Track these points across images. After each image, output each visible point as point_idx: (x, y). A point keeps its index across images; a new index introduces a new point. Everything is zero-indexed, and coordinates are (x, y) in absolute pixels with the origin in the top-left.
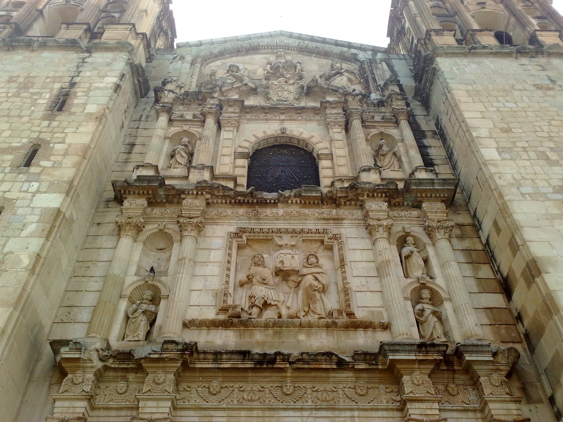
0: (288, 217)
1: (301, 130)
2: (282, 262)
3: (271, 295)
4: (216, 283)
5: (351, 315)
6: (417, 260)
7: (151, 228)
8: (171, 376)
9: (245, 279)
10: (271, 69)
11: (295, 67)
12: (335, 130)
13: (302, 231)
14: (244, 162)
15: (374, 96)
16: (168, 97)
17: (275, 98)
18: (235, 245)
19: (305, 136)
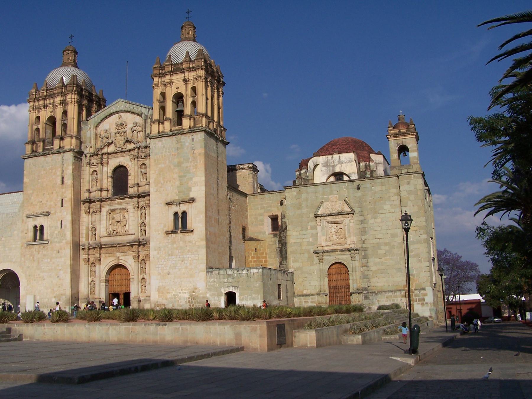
0: (118, 203)
1: (124, 161)
3: (115, 228)
4: (105, 225)
5: (128, 232)
6: (143, 214)
7: (91, 211)
8: (99, 249)
9: (110, 223)
10: (117, 126)
11: (124, 125)
12: (132, 162)
13: (121, 209)
14: (110, 180)
15: (143, 144)
16: (88, 157)
17: (118, 145)
18: (108, 213)
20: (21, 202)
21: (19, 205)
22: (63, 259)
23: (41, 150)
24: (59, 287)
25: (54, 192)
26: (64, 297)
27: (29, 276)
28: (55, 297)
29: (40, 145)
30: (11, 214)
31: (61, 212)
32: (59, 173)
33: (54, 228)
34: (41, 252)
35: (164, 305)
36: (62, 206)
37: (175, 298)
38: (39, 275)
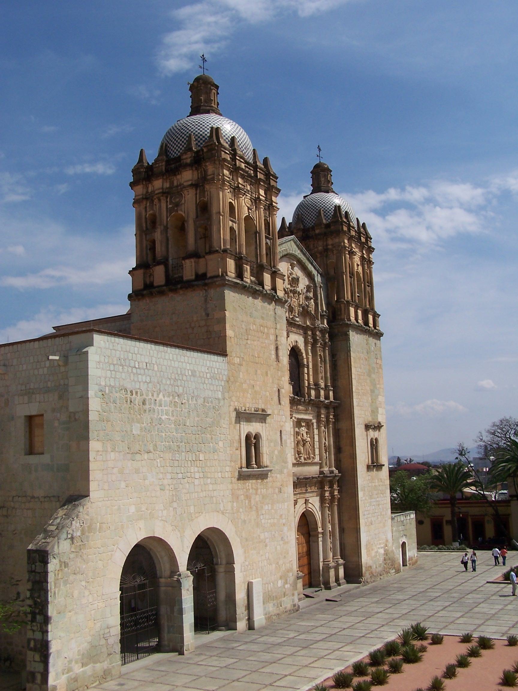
2: (302, 434)
19: (301, 349)
20: (224, 379)
21: (223, 383)
22: (286, 504)
23: (249, 281)
24: (285, 557)
25: (269, 372)
26: (291, 574)
27: (247, 540)
28: (281, 578)
29: (247, 268)
30: (212, 402)
31: (278, 415)
32: (272, 338)
33: (272, 444)
34: (259, 491)
35: (371, 567)
36: (280, 404)
37: (377, 556)
38: (259, 536)
